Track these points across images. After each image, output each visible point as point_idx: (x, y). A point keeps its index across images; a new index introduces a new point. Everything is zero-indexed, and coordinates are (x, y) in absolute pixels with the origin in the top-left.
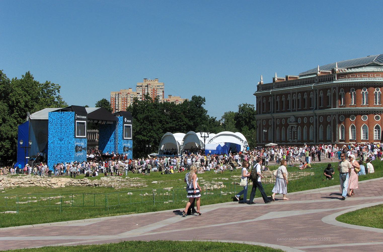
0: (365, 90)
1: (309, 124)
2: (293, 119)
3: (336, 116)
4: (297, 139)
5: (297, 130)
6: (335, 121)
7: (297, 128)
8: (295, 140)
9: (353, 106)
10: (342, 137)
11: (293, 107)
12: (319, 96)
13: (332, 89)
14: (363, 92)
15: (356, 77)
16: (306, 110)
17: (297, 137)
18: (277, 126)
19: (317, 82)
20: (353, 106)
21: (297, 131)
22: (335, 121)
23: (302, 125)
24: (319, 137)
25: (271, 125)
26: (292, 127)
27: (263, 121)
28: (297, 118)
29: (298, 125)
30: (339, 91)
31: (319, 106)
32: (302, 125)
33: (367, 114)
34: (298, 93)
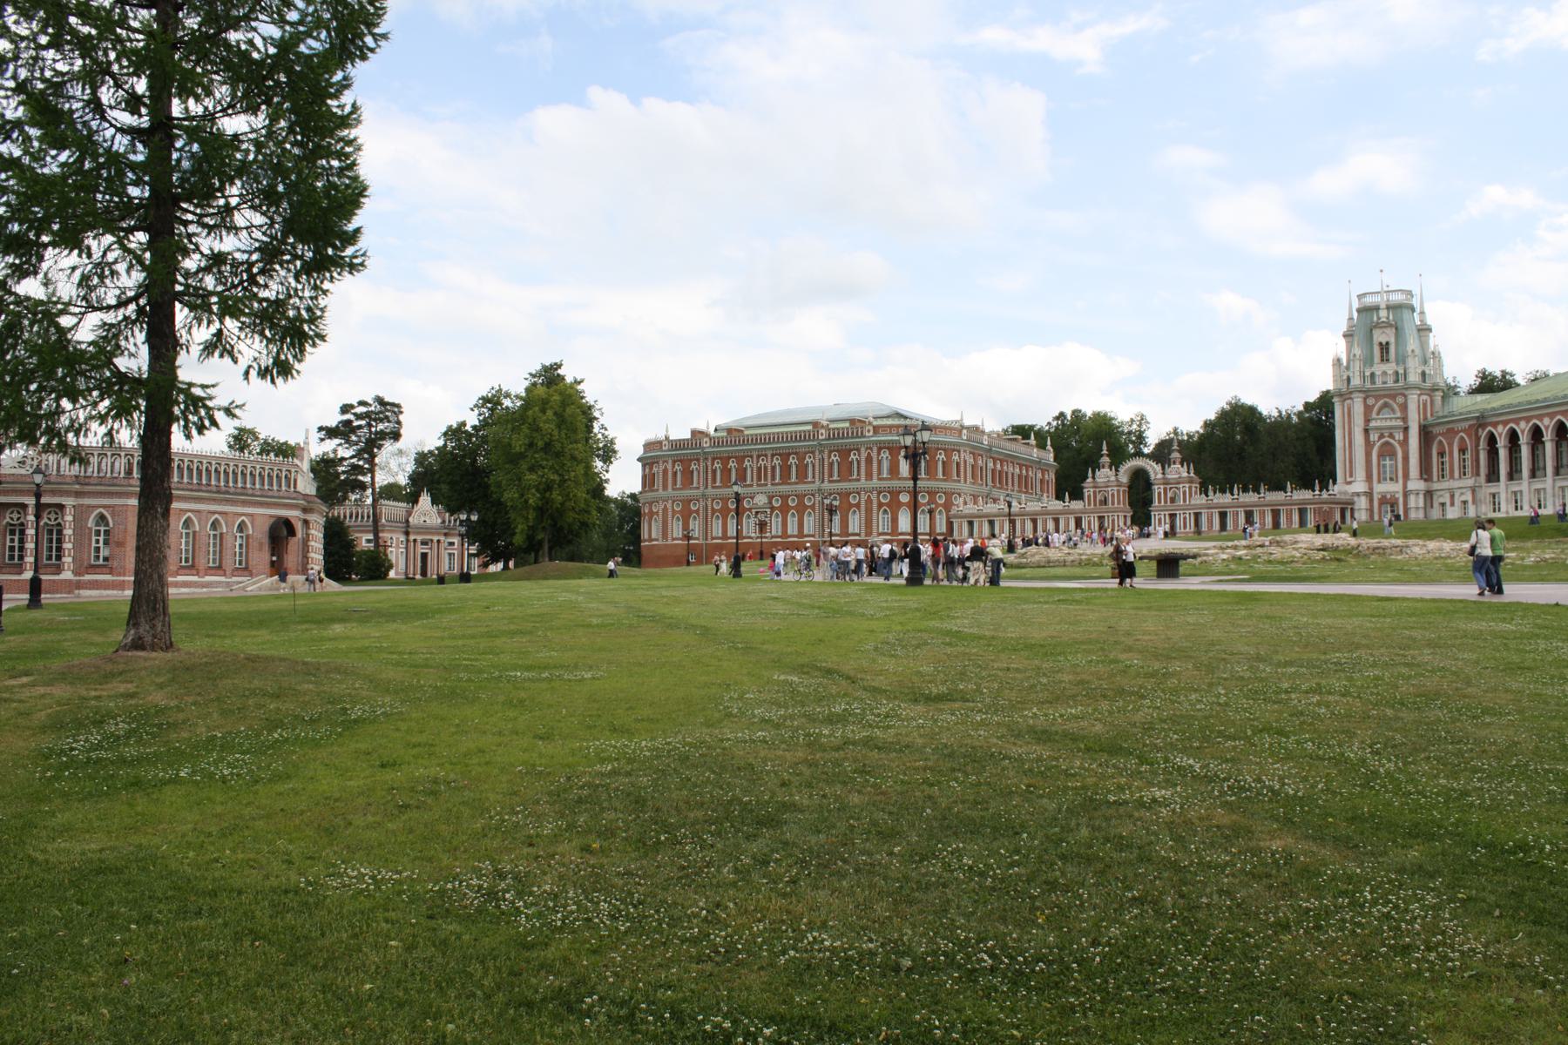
1: (801, 509)
2: (761, 500)
6: (869, 501)
11: (759, 479)
18: (714, 511)
22: (869, 501)
28: (770, 498)
29: (773, 509)
32: (784, 510)
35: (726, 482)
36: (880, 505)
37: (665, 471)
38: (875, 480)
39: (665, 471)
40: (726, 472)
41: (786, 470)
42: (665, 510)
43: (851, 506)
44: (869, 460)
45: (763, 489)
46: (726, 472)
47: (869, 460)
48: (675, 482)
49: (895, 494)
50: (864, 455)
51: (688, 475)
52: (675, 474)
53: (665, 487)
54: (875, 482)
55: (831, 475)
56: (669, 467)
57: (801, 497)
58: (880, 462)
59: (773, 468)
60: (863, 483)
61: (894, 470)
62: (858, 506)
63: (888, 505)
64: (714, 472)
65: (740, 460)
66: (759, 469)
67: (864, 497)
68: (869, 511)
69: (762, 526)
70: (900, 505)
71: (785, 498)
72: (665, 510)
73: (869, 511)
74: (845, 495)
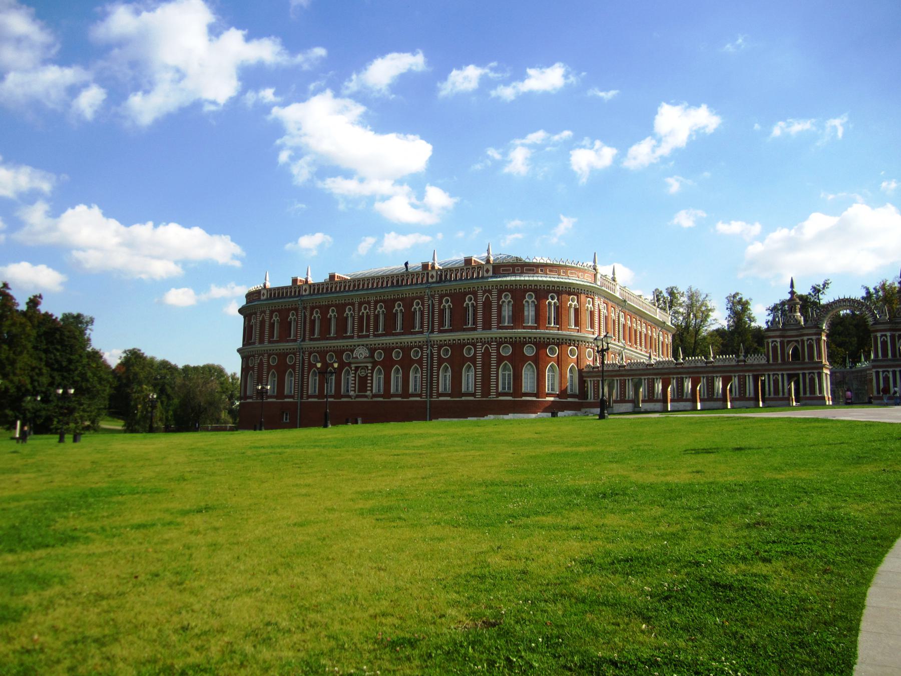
0: (553, 298)
1: (406, 364)
2: (361, 353)
3: (490, 345)
4: (371, 391)
5: (372, 373)
6: (487, 355)
7: (373, 370)
8: (369, 393)
9: (530, 327)
10: (504, 388)
11: (361, 329)
12: (439, 307)
13: (480, 293)
14: (550, 303)
15: (537, 273)
16: (402, 334)
17: (372, 387)
19: (434, 280)
20: (530, 327)
21: (372, 377)
22: (487, 355)
23: (387, 365)
24: (438, 388)
25: (253, 367)
26: (357, 368)
27: (269, 358)
28: (372, 351)
29: (375, 364)
30: (499, 298)
31: (439, 328)
32: (387, 365)
33: (558, 345)
34: (376, 302)
35: (325, 334)
36: (500, 359)
37: (263, 323)
38: (494, 330)
39: (263, 323)
40: (326, 322)
41: (390, 319)
42: (261, 364)
43: (464, 360)
44: (487, 305)
45: (364, 341)
46: (326, 322)
47: (487, 305)
48: (271, 335)
49: (518, 345)
50: (481, 299)
51: (286, 327)
52: (272, 326)
53: (261, 341)
54: (495, 333)
55: (442, 323)
56: (267, 318)
57: (406, 349)
58: (500, 308)
59: (377, 317)
60: (480, 334)
61: (518, 318)
62: (473, 360)
63: (511, 359)
64: (313, 322)
65: (341, 308)
66: (361, 318)
67: (481, 350)
68: (486, 367)
69: (363, 384)
70: (525, 359)
71: (388, 350)
72: (261, 364)
73: (486, 367)
74: (457, 347)
